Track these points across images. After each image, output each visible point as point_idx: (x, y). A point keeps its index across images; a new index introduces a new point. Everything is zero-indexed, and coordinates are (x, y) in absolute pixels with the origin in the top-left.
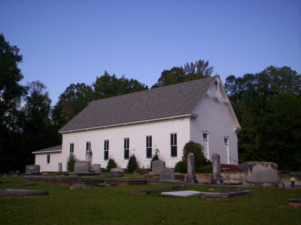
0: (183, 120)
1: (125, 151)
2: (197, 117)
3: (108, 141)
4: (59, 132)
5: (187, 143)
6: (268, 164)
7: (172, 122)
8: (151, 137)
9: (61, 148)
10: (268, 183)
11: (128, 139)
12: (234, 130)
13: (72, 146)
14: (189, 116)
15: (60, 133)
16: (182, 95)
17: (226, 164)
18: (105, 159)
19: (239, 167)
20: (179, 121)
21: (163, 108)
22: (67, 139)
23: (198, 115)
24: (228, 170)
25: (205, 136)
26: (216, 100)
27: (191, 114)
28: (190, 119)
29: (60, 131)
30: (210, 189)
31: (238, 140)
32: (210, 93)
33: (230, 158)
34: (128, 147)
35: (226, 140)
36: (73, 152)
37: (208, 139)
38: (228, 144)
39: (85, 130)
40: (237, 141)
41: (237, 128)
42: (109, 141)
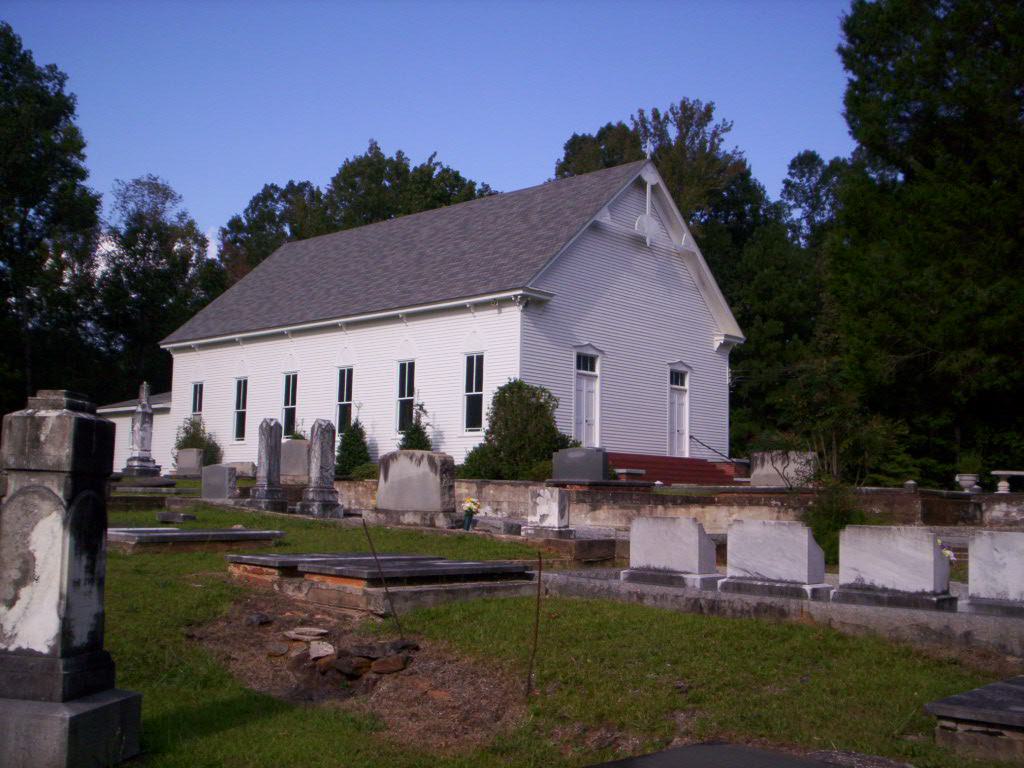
0: (504, 310)
1: (238, 413)
2: (548, 301)
3: (295, 377)
4: (162, 347)
5: (501, 385)
6: (422, 456)
7: (471, 315)
8: (412, 365)
9: (169, 399)
10: (415, 512)
11: (350, 372)
12: (717, 345)
13: (198, 389)
14: (516, 296)
15: (164, 350)
16: (525, 226)
17: (677, 455)
18: (237, 436)
19: (719, 467)
20: (491, 312)
21: (456, 269)
22: (186, 369)
23: (552, 295)
24: (641, 475)
25: (586, 362)
26: (639, 242)
27: (521, 292)
28: (521, 307)
29: (164, 344)
30: (235, 527)
31: (732, 378)
32: (608, 218)
33: (691, 437)
34: (349, 398)
35: (677, 378)
36: (200, 409)
37: (597, 372)
38: (686, 391)
39: (232, 342)
40: (728, 381)
41: (726, 336)
42: (298, 377)
